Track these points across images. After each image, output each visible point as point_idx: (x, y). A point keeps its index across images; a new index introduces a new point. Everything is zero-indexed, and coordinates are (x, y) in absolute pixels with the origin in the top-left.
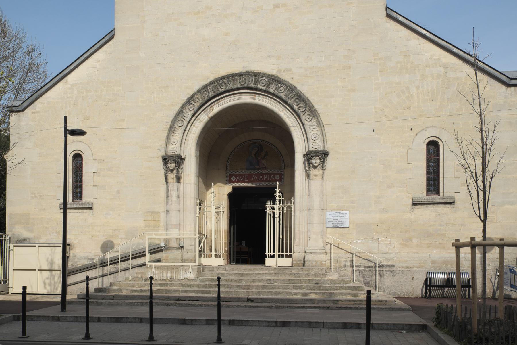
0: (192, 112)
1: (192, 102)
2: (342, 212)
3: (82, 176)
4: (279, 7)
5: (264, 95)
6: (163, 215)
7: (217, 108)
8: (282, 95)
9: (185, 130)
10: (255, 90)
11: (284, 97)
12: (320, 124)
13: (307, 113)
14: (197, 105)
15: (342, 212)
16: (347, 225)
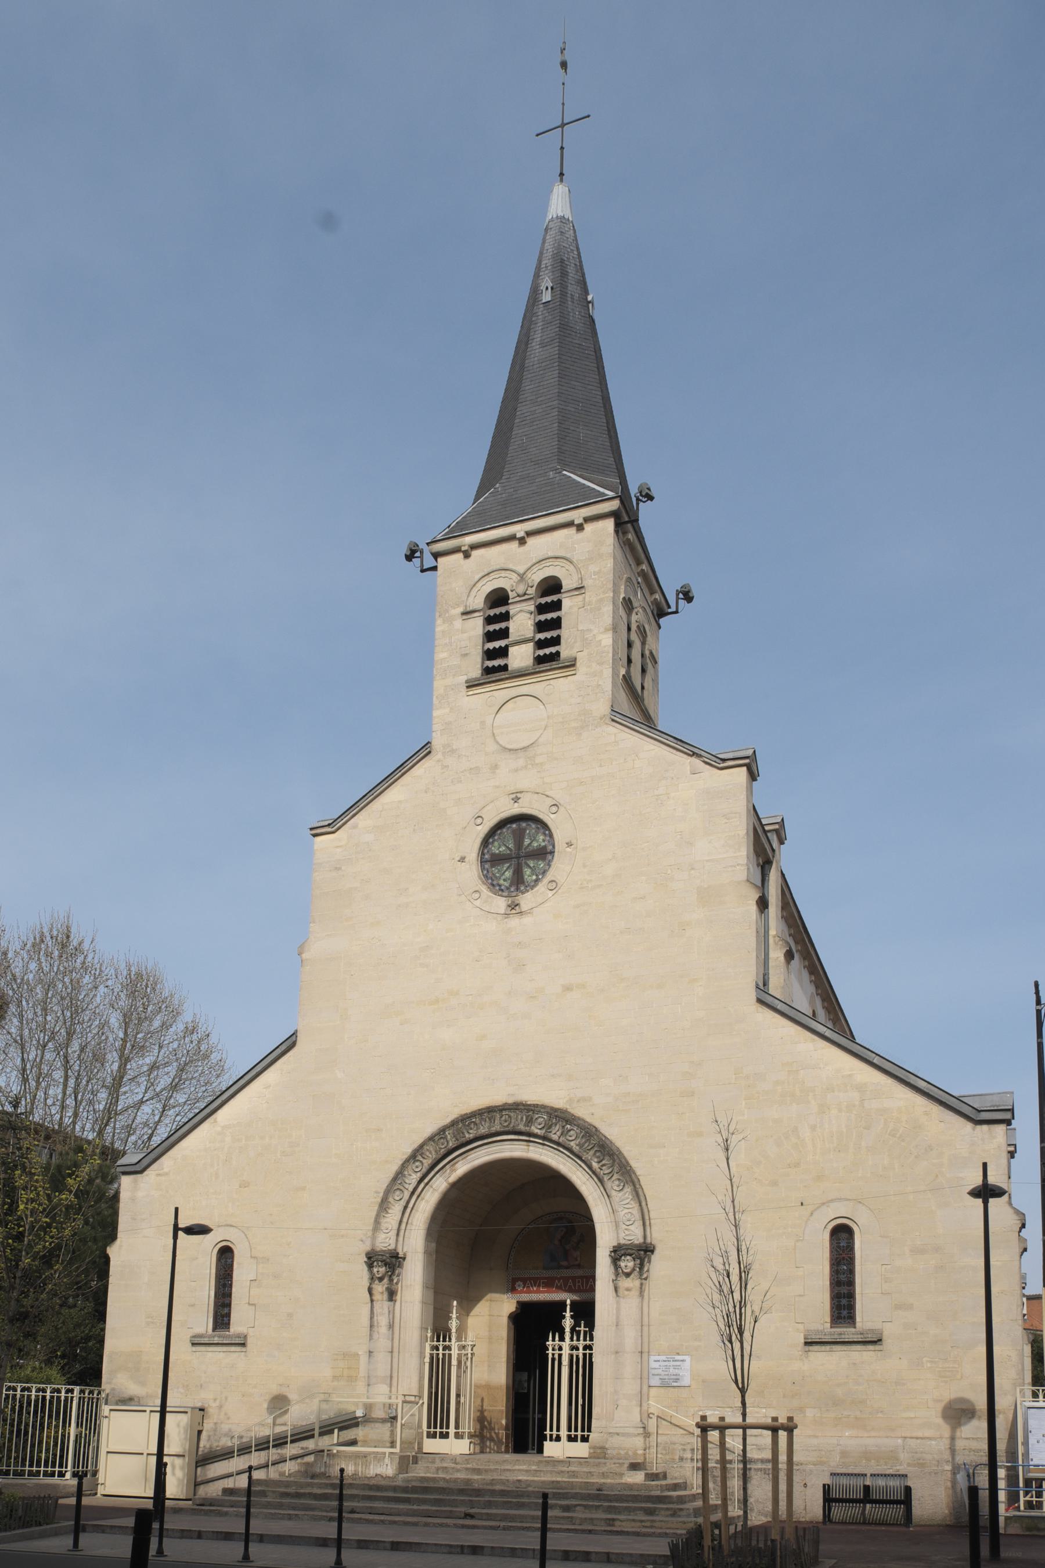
0: (419, 1175)
1: (419, 1158)
3: (231, 1286)
4: (572, 990)
6: (364, 1359)
7: (462, 1167)
9: (406, 1207)
10: (529, 1136)
11: (576, 1149)
12: (638, 1195)
13: (616, 1176)
14: (427, 1163)
16: (686, 1381)
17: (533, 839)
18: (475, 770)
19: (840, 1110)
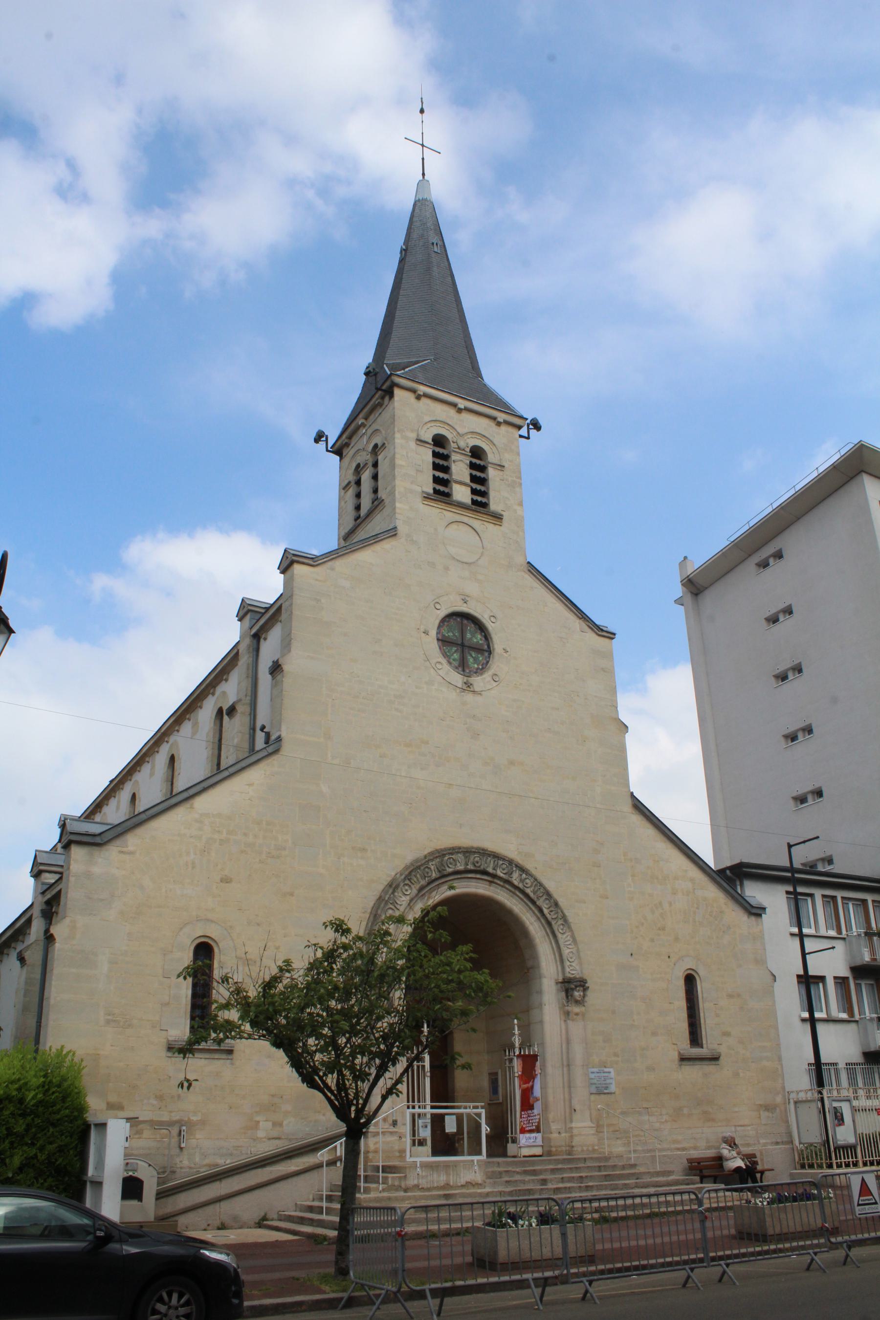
0: (408, 898)
1: (407, 882)
2: (606, 1070)
5: (502, 886)
8: (528, 891)
11: (532, 895)
15: (606, 1070)
16: (613, 1088)
17: (473, 636)
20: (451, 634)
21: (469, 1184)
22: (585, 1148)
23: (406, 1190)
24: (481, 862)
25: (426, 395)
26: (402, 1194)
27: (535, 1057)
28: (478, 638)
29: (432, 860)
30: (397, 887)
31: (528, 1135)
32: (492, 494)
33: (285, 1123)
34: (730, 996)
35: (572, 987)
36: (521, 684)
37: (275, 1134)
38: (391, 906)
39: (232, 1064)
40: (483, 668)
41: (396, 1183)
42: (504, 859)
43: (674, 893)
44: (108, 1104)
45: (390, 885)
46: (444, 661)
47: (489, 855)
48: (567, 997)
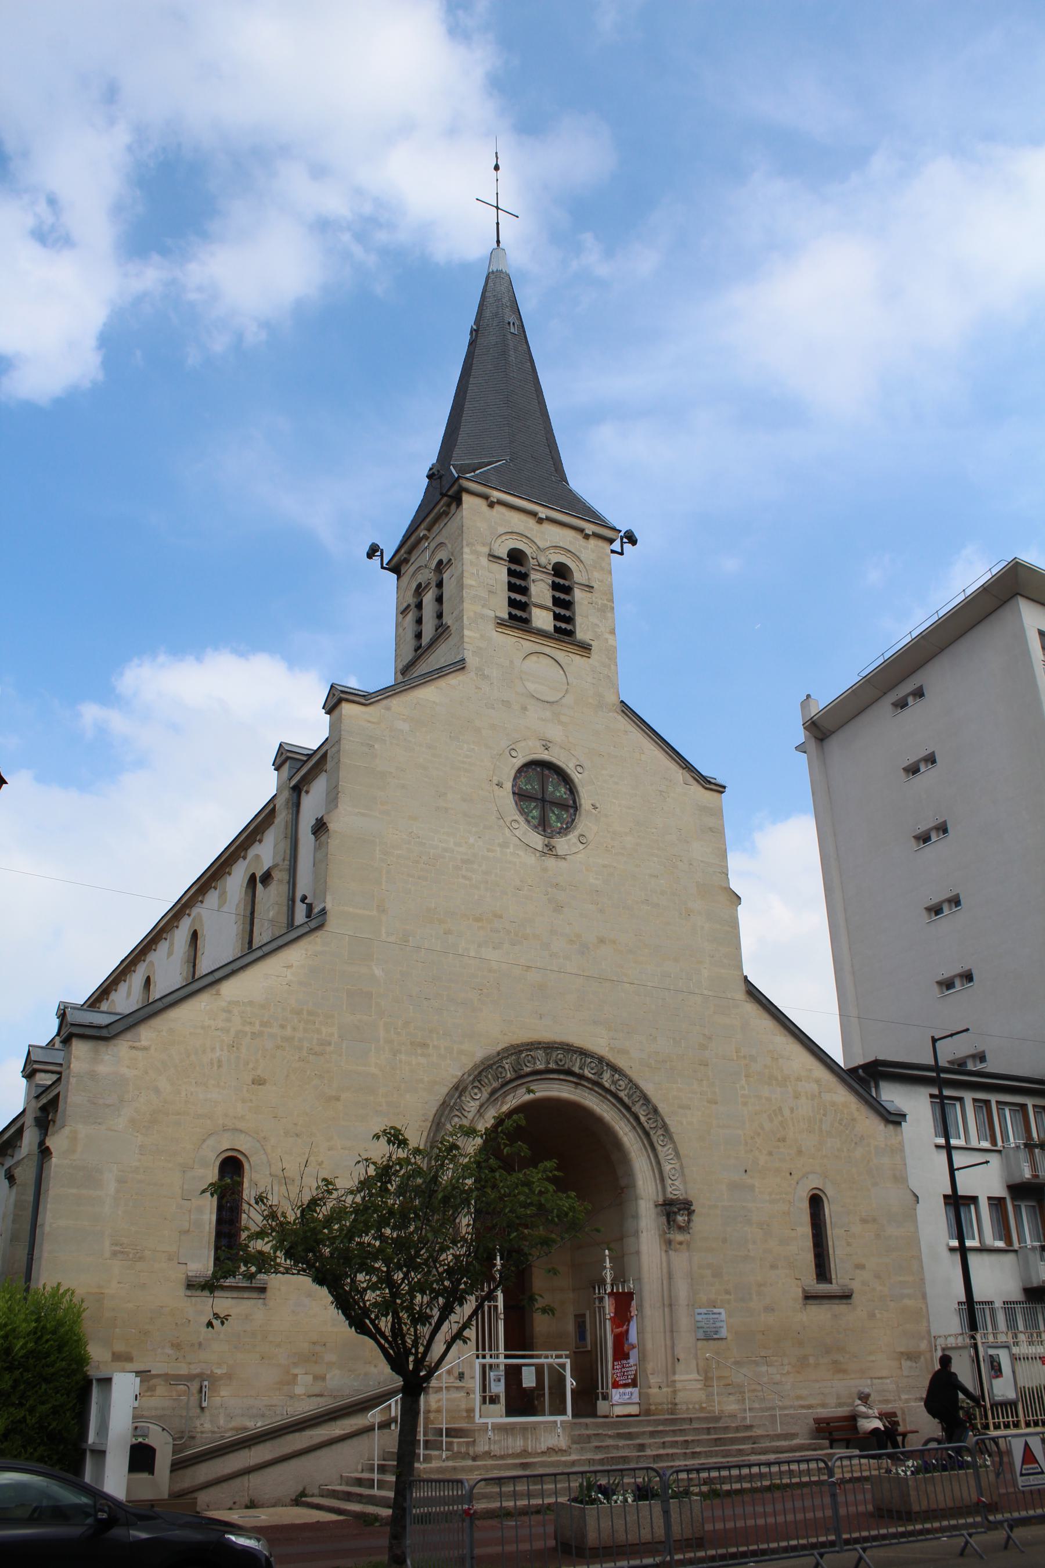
0: (478, 1103)
1: (477, 1084)
2: (716, 1310)
8: (622, 1094)
11: (626, 1099)
15: (716, 1310)
17: (556, 788)
18: (506, 704)
19: (807, 1098)
20: (529, 787)
21: (551, 1451)
22: (691, 1406)
23: (474, 1459)
24: (564, 1060)
25: (500, 502)
26: (470, 1463)
27: (630, 1296)
28: (562, 792)
29: (507, 1058)
30: (465, 1089)
31: (622, 1390)
32: (579, 620)
33: (328, 1376)
34: (864, 1221)
35: (675, 1211)
36: (613, 847)
37: (316, 1390)
38: (457, 1113)
39: (265, 1304)
40: (567, 828)
41: (463, 1450)
42: (593, 1057)
43: (797, 1096)
44: (114, 1354)
45: (456, 1087)
46: (521, 819)
47: (575, 1052)
48: (669, 1222)
